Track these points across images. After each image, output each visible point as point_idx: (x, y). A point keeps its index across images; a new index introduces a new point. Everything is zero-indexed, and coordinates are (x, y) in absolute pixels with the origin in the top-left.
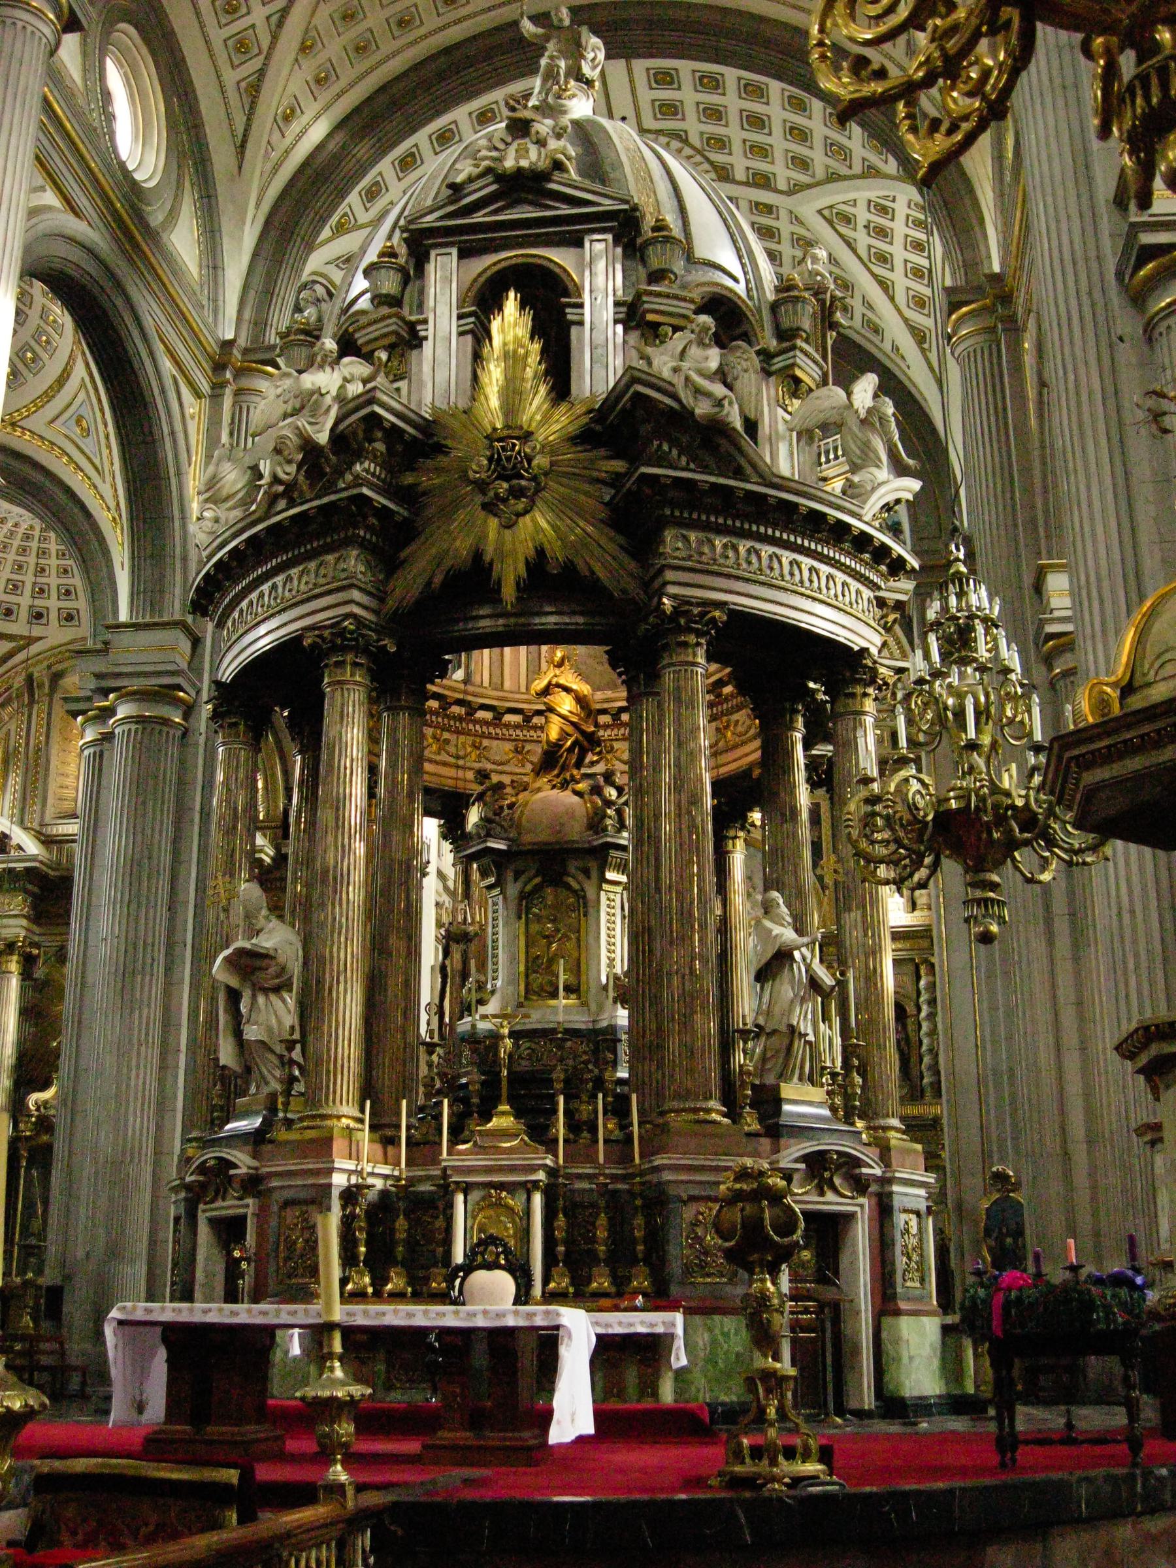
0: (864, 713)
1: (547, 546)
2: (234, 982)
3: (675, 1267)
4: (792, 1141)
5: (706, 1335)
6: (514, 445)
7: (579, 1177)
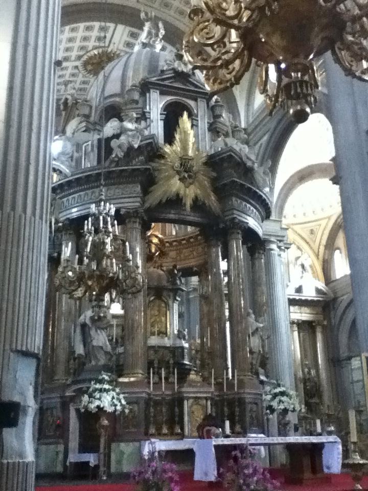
0: (262, 259)
1: (198, 197)
6: (189, 162)
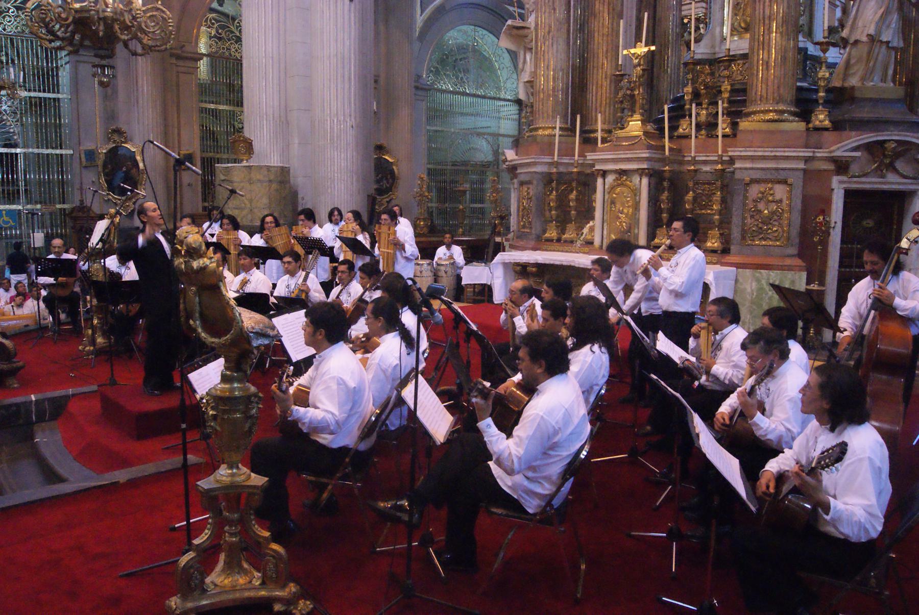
2: (512, 47)
3: (736, 233)
4: (854, 133)
5: (754, 284)
7: (705, 162)
